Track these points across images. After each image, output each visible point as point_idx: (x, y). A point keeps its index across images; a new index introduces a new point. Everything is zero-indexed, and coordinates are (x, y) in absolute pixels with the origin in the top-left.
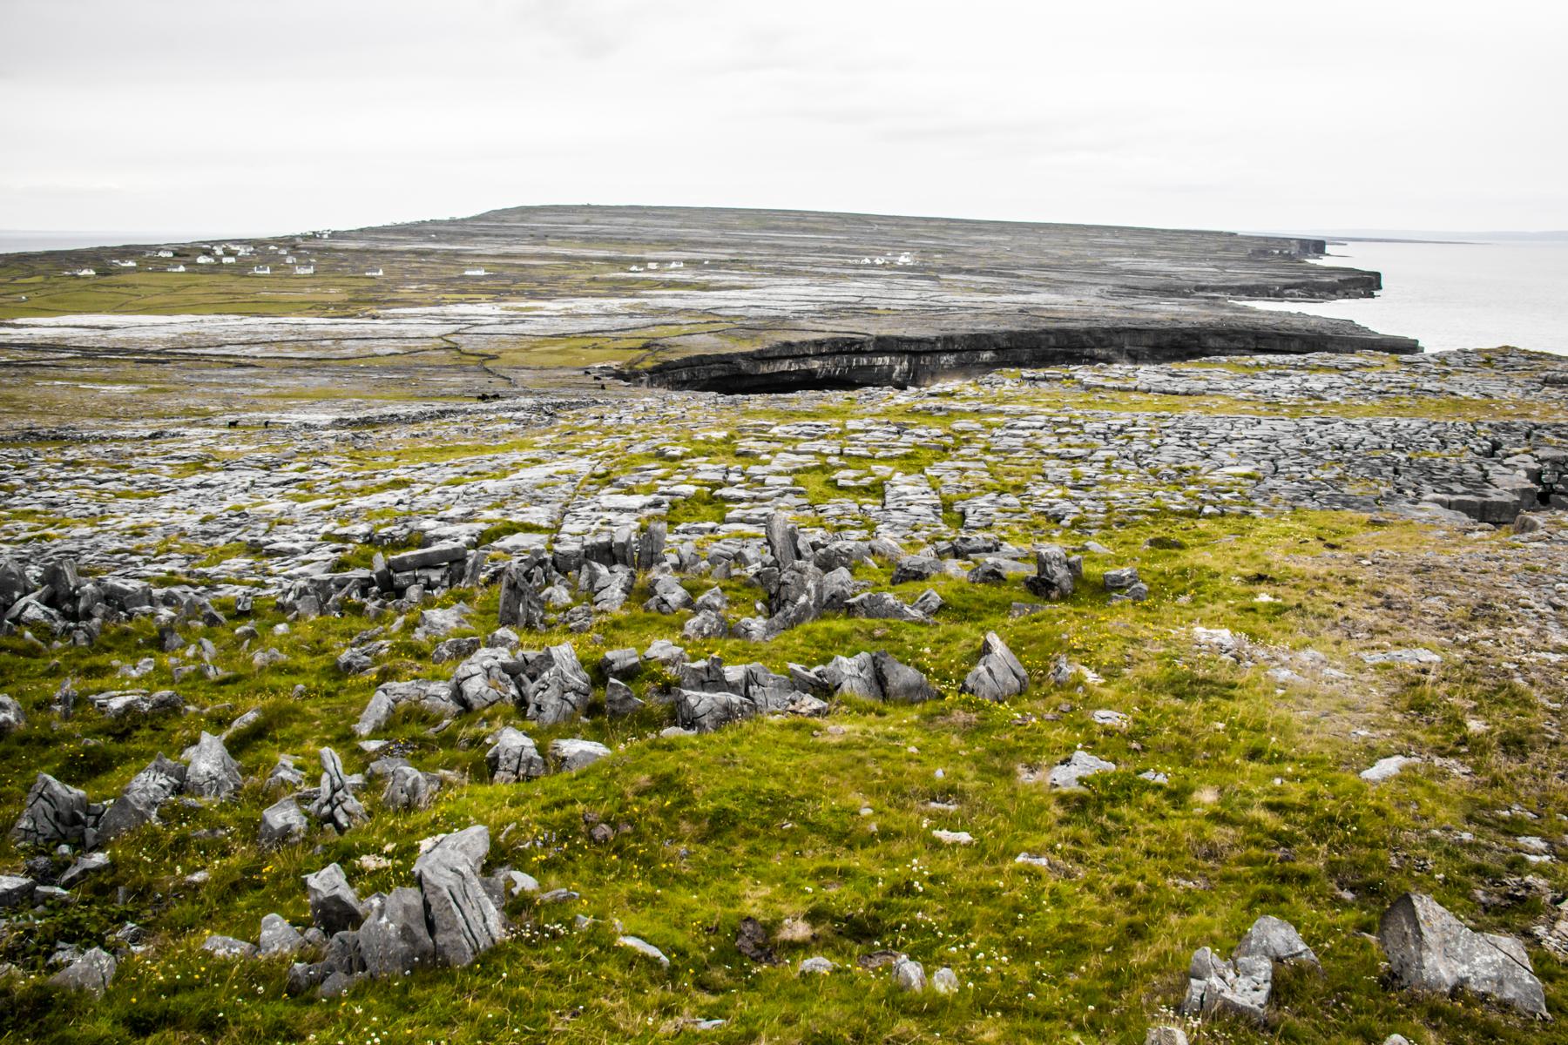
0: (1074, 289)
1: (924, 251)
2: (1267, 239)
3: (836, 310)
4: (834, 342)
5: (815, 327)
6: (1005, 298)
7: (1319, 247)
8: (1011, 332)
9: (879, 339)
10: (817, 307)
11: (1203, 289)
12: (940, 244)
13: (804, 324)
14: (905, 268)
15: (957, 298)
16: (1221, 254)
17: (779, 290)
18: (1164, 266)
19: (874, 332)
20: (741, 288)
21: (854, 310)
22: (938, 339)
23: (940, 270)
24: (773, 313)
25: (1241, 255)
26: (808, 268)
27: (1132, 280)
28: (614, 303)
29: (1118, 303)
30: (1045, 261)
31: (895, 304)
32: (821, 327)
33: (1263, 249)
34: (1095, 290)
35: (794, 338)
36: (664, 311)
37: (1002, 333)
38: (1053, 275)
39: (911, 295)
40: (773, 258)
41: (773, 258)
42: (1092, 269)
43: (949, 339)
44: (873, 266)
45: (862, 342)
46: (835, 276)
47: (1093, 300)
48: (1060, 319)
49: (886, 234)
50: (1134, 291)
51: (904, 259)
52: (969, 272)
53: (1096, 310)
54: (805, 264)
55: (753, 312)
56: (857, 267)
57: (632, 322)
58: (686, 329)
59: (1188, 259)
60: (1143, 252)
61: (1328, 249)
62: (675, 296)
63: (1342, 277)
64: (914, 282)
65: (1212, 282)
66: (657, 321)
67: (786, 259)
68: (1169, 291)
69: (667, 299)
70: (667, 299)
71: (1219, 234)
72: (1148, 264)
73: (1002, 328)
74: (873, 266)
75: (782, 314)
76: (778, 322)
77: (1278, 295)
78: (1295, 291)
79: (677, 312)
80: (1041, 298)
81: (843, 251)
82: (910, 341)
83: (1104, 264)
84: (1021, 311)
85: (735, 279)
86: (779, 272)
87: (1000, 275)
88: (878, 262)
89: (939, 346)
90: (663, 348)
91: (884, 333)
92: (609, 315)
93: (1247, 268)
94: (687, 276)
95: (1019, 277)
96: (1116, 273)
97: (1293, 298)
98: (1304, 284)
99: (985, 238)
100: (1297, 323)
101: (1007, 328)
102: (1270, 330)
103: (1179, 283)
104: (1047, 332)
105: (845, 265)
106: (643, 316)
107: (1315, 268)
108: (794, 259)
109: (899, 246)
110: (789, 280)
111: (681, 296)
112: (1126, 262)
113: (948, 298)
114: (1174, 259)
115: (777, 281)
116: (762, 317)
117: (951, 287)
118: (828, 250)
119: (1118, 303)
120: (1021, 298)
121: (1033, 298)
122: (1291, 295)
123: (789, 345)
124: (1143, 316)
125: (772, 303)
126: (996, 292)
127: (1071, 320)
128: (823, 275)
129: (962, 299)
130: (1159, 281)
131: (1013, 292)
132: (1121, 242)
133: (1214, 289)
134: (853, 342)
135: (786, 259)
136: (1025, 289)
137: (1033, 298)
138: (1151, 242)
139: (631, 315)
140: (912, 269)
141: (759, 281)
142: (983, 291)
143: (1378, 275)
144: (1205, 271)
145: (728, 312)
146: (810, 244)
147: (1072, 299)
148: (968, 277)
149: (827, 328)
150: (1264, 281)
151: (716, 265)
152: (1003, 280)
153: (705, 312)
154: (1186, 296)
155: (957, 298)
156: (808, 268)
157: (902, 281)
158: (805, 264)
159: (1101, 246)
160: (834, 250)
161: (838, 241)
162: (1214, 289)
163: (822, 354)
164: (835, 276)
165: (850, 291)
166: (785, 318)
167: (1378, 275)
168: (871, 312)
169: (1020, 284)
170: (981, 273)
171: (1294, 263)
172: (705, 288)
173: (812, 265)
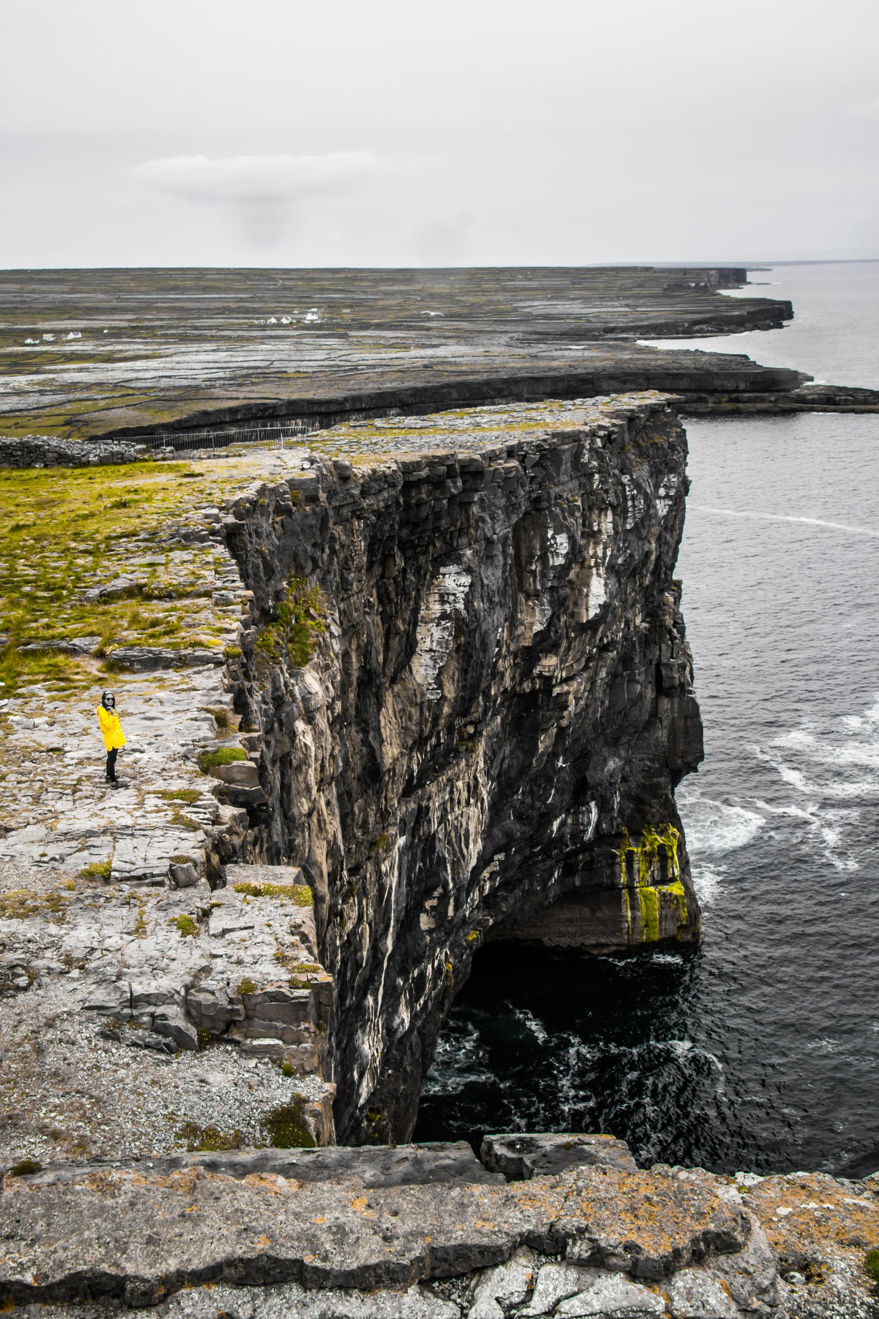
0: (483, 339)
1: (332, 306)
2: (685, 271)
3: (248, 376)
4: (248, 408)
5: (228, 394)
6: (414, 352)
7: (737, 276)
8: (416, 389)
9: (291, 403)
10: (228, 374)
11: (612, 330)
12: (348, 298)
13: (218, 392)
14: (313, 326)
15: (367, 356)
16: (636, 291)
17: (187, 358)
18: (576, 308)
19: (285, 397)
20: (146, 357)
21: (263, 375)
22: (346, 399)
23: (349, 327)
24: (185, 383)
25: (657, 291)
26: (214, 332)
27: (542, 326)
28: (20, 381)
29: (524, 352)
30: (456, 310)
31: (305, 366)
32: (235, 395)
33: (680, 283)
34: (505, 339)
35: (211, 406)
36: (73, 386)
37: (406, 390)
38: (465, 325)
39: (320, 355)
40: (175, 323)
41: (175, 323)
42: (501, 317)
43: (356, 399)
44: (279, 326)
45: (274, 407)
46: (241, 339)
47: (503, 349)
48: (462, 373)
49: (290, 289)
50: (544, 337)
51: (310, 317)
52: (379, 327)
53: (498, 360)
54: (209, 328)
55: (164, 383)
56: (264, 327)
57: (46, 399)
58: (102, 404)
59: (602, 299)
60: (557, 294)
61: (750, 276)
62: (80, 370)
63: (752, 309)
64: (322, 341)
65: (621, 322)
66: (71, 397)
67: (189, 323)
68: (577, 335)
69: (72, 374)
70: (72, 374)
71: (634, 269)
72: (562, 307)
73: (407, 385)
74: (279, 326)
75: (193, 383)
76: (191, 392)
77: (688, 332)
78: (704, 327)
79: (88, 387)
80: (449, 351)
81: (247, 311)
82: (320, 403)
83: (515, 309)
84: (426, 366)
85: (137, 347)
86: (184, 339)
87: (409, 328)
88: (284, 321)
89: (348, 406)
90: (86, 423)
91: (295, 397)
92: (19, 393)
93: (659, 305)
94: (88, 347)
95: (428, 329)
96: (527, 319)
97: (703, 334)
98: (712, 319)
99: (395, 288)
100: (688, 362)
101: (411, 384)
102: (660, 370)
103: (590, 326)
104: (449, 386)
105: (251, 327)
106: (54, 392)
107: (728, 301)
108: (198, 323)
109: (306, 303)
110: (195, 347)
111: (87, 370)
112: (539, 306)
113: (358, 356)
114: (586, 300)
115: (183, 348)
116: (175, 388)
117: (359, 344)
118: (231, 311)
119: (524, 352)
120: (429, 352)
121: (441, 352)
122: (699, 331)
123: (206, 413)
124: (542, 364)
125: (182, 373)
126: (407, 348)
127: (473, 373)
128: (229, 338)
129: (370, 357)
130: (571, 324)
131: (424, 346)
132: (533, 284)
133: (624, 330)
134: (266, 407)
135: (189, 323)
136: (435, 342)
137: (441, 352)
138: (566, 282)
139: (42, 393)
140: (320, 327)
141: (164, 349)
142: (392, 346)
143: (788, 304)
144: (614, 311)
145: (139, 384)
146: (212, 305)
147: (480, 350)
148: (377, 333)
149: (241, 395)
150: (673, 318)
151: (117, 334)
152: (413, 334)
153: (116, 386)
154: (595, 338)
155: (367, 356)
156: (214, 332)
157: (310, 340)
158: (209, 328)
159: (515, 290)
160: (238, 310)
161: (242, 300)
162: (624, 330)
163: (238, 421)
164: (241, 339)
165: (257, 355)
166: (197, 388)
167: (788, 304)
168: (281, 377)
169: (429, 337)
170: (390, 327)
171: (706, 296)
172: (110, 358)
173: (217, 328)
